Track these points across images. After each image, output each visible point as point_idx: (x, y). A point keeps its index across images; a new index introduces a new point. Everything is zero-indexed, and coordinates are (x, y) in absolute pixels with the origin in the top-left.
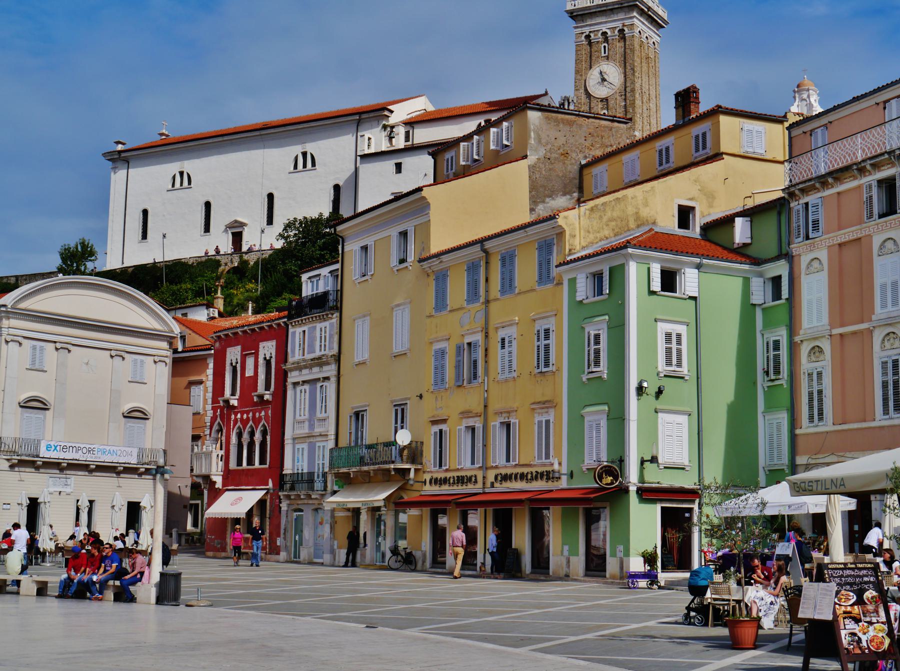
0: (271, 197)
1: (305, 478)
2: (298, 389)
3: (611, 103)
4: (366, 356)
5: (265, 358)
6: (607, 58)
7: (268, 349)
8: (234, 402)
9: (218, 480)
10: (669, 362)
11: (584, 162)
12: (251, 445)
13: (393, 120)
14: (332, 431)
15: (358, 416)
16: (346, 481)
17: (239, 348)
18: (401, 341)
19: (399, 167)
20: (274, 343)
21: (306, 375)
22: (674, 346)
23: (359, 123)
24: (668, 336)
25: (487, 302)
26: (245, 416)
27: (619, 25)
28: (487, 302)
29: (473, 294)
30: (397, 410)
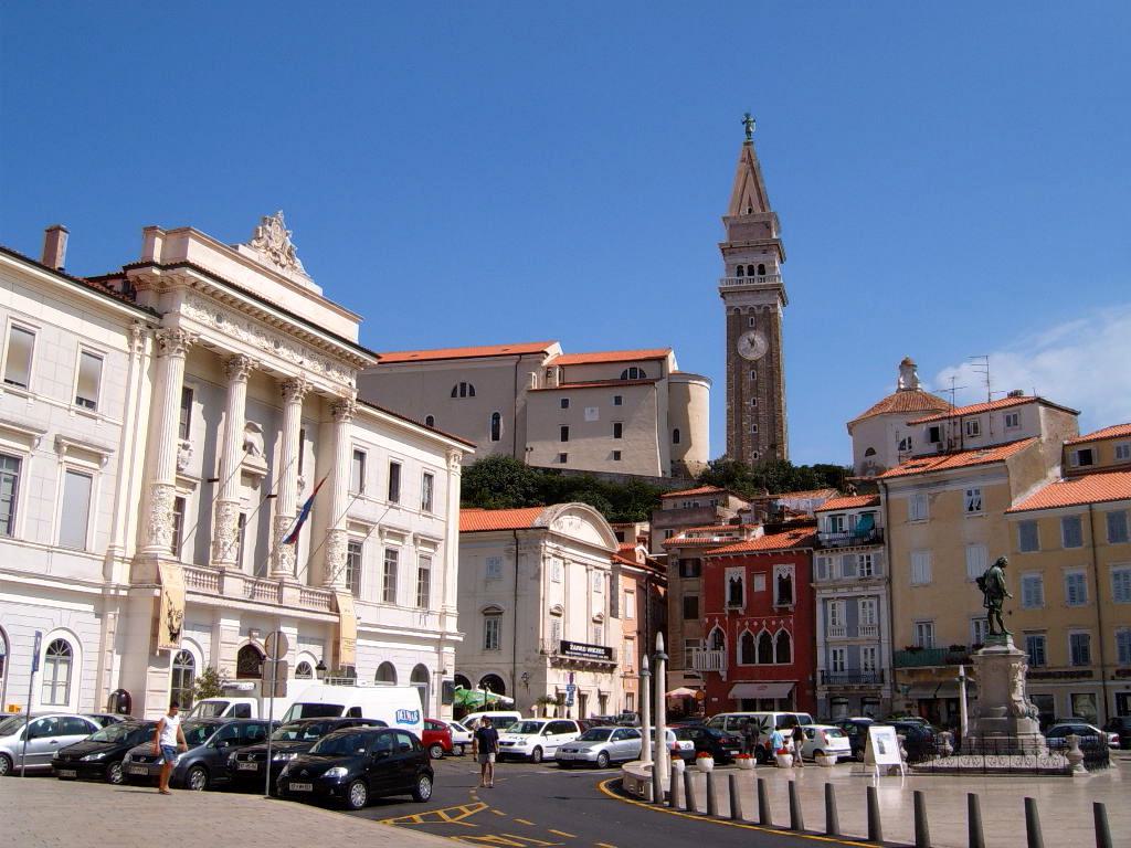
1: (846, 673)
2: (830, 604)
3: (760, 363)
4: (928, 578)
5: (780, 577)
6: (755, 329)
8: (741, 612)
9: (723, 674)
11: (1066, 442)
13: (545, 363)
17: (743, 568)
19: (565, 404)
20: (793, 566)
25: (1094, 546)
26: (756, 624)
28: (1094, 546)
30: (977, 624)
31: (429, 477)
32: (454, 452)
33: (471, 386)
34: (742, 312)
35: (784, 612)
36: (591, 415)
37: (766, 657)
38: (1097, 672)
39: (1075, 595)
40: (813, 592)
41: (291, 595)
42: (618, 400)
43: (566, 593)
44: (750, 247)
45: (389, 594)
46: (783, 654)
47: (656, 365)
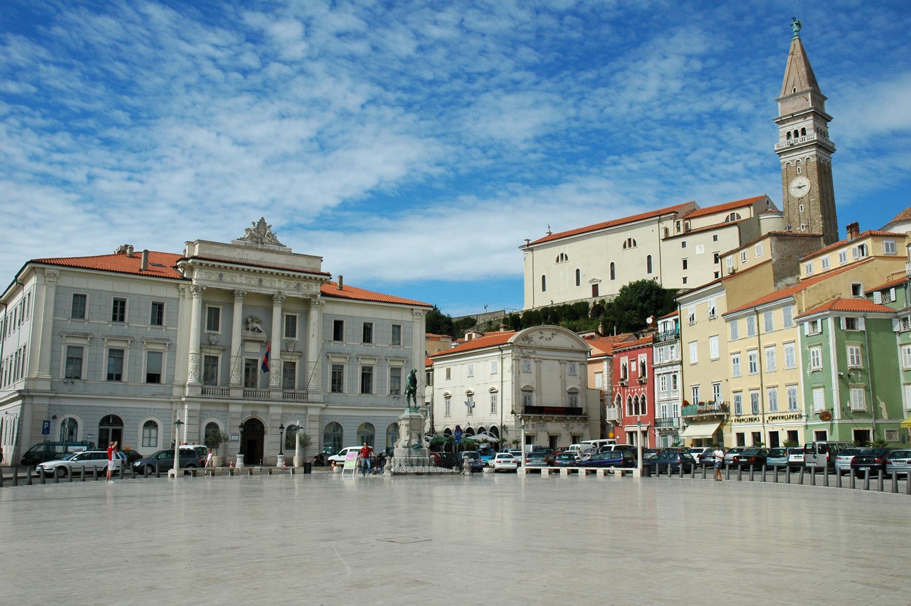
0: (612, 264)
6: (800, 175)
7: (643, 357)
10: (853, 363)
12: (637, 405)
14: (680, 397)
15: (695, 389)
16: (690, 421)
18: (714, 354)
19: (684, 244)
21: (665, 370)
22: (855, 355)
23: (659, 221)
24: (852, 350)
25: (759, 335)
27: (807, 155)
28: (759, 335)
29: (751, 332)
31: (397, 328)
32: (414, 311)
33: (634, 241)
34: (793, 165)
35: (641, 383)
36: (700, 250)
37: (637, 413)
38: (761, 417)
39: (753, 368)
40: (654, 369)
41: (274, 394)
42: (715, 238)
43: (539, 378)
44: (793, 117)
45: (366, 387)
46: (643, 412)
47: (747, 209)
